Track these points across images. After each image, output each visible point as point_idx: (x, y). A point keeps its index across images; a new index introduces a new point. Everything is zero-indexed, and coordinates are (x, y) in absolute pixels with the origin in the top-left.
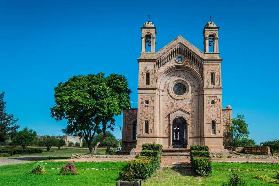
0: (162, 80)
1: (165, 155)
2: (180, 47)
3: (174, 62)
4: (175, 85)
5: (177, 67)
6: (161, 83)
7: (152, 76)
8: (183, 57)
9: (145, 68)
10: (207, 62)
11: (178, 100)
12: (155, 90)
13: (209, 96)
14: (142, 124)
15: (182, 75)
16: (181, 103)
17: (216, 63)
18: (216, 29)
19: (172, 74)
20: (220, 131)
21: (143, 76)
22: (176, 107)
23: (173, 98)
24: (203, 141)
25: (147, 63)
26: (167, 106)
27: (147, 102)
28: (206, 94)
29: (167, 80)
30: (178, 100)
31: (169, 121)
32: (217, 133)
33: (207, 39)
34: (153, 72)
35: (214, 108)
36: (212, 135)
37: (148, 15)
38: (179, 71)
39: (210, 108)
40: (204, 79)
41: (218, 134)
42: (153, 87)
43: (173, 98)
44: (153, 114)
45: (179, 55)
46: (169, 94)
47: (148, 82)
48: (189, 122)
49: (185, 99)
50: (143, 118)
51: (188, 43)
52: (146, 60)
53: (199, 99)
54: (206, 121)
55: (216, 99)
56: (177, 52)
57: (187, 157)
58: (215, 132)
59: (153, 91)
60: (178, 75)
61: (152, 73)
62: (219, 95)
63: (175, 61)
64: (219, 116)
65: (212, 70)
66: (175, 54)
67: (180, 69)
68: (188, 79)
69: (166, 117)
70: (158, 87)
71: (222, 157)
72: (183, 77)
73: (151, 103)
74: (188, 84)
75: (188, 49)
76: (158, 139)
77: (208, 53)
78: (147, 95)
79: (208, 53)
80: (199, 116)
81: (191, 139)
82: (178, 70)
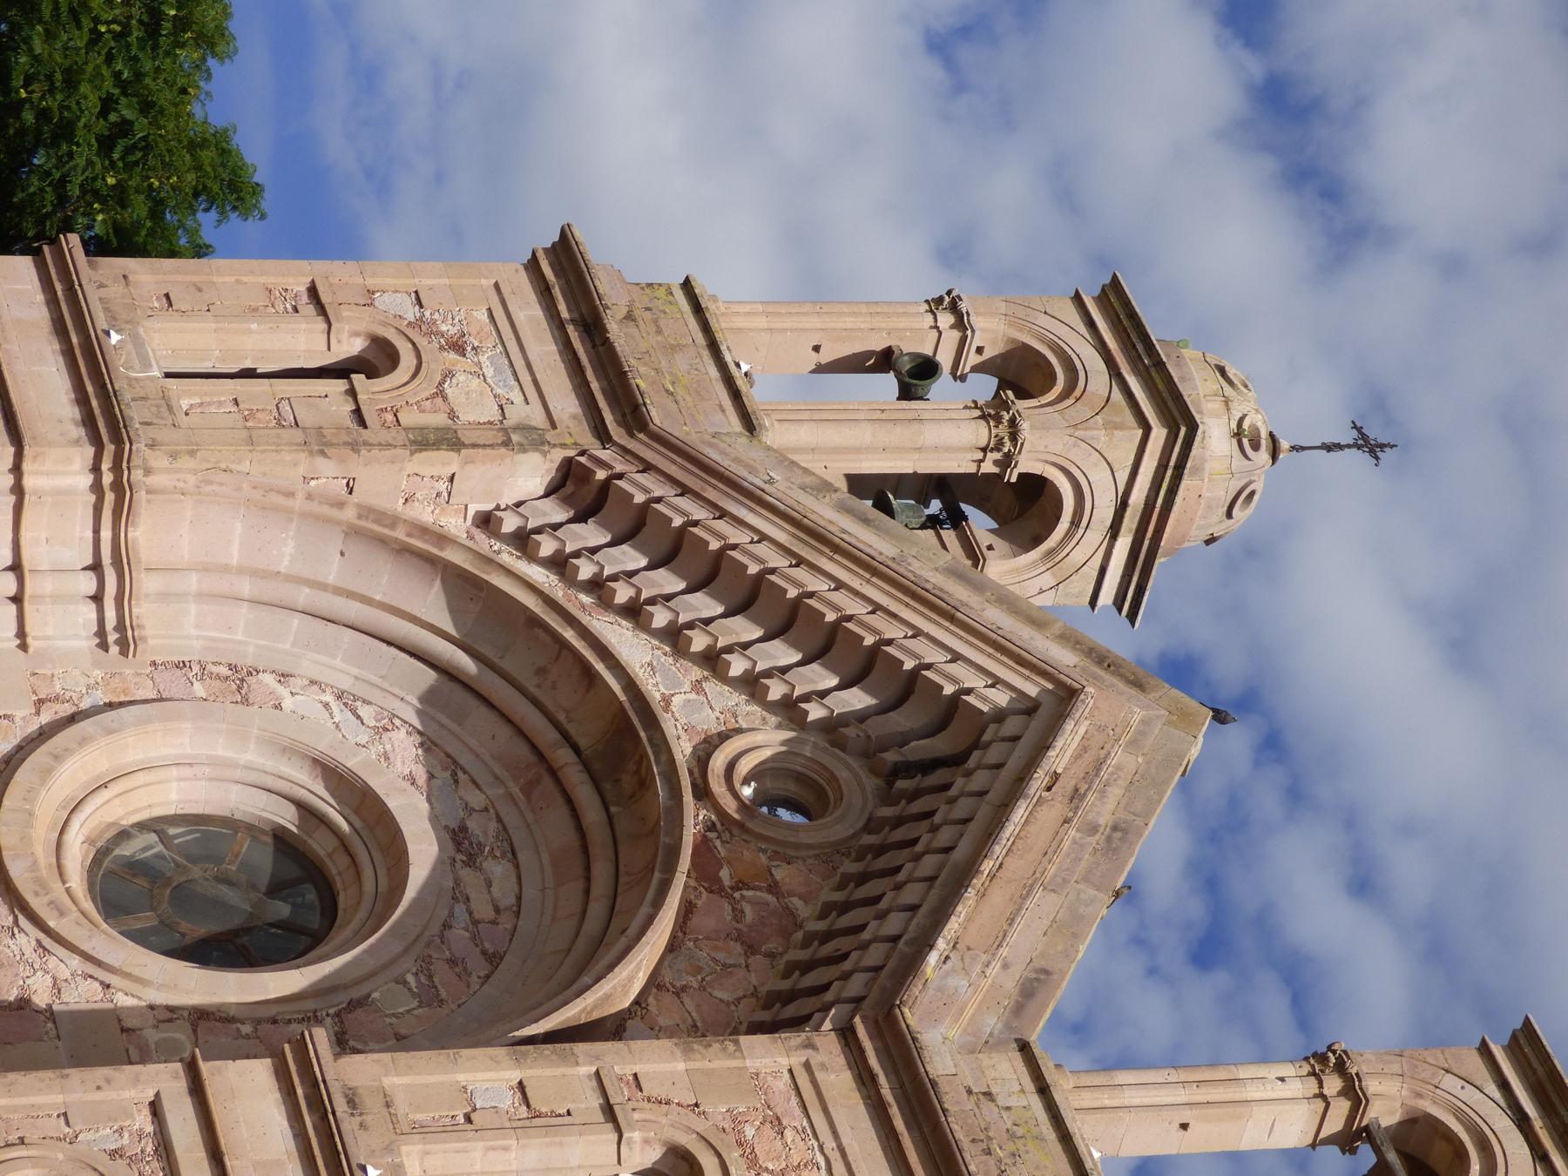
2: (999, 716)
3: (709, 722)
4: (280, 837)
6: (245, 587)
8: (837, 828)
10: (865, 1079)
12: (81, 432)
15: (504, 891)
21: (310, 310)
25: (544, 350)
28: (197, 1089)
29: (345, 683)
33: (1333, 1084)
34: (409, 418)
37: (1375, 433)
38: (558, 816)
42: (136, 414)
46: (72, 719)
49: (27, 940)
51: (1104, 808)
52: (592, 325)
56: (900, 720)
59: (72, 412)
61: (385, 401)
63: (723, 737)
65: (733, 1157)
66: (857, 699)
67: (592, 814)
68: (452, 962)
72: (459, 895)
77: (1043, 1090)
79: (1043, 1090)
82: (577, 779)
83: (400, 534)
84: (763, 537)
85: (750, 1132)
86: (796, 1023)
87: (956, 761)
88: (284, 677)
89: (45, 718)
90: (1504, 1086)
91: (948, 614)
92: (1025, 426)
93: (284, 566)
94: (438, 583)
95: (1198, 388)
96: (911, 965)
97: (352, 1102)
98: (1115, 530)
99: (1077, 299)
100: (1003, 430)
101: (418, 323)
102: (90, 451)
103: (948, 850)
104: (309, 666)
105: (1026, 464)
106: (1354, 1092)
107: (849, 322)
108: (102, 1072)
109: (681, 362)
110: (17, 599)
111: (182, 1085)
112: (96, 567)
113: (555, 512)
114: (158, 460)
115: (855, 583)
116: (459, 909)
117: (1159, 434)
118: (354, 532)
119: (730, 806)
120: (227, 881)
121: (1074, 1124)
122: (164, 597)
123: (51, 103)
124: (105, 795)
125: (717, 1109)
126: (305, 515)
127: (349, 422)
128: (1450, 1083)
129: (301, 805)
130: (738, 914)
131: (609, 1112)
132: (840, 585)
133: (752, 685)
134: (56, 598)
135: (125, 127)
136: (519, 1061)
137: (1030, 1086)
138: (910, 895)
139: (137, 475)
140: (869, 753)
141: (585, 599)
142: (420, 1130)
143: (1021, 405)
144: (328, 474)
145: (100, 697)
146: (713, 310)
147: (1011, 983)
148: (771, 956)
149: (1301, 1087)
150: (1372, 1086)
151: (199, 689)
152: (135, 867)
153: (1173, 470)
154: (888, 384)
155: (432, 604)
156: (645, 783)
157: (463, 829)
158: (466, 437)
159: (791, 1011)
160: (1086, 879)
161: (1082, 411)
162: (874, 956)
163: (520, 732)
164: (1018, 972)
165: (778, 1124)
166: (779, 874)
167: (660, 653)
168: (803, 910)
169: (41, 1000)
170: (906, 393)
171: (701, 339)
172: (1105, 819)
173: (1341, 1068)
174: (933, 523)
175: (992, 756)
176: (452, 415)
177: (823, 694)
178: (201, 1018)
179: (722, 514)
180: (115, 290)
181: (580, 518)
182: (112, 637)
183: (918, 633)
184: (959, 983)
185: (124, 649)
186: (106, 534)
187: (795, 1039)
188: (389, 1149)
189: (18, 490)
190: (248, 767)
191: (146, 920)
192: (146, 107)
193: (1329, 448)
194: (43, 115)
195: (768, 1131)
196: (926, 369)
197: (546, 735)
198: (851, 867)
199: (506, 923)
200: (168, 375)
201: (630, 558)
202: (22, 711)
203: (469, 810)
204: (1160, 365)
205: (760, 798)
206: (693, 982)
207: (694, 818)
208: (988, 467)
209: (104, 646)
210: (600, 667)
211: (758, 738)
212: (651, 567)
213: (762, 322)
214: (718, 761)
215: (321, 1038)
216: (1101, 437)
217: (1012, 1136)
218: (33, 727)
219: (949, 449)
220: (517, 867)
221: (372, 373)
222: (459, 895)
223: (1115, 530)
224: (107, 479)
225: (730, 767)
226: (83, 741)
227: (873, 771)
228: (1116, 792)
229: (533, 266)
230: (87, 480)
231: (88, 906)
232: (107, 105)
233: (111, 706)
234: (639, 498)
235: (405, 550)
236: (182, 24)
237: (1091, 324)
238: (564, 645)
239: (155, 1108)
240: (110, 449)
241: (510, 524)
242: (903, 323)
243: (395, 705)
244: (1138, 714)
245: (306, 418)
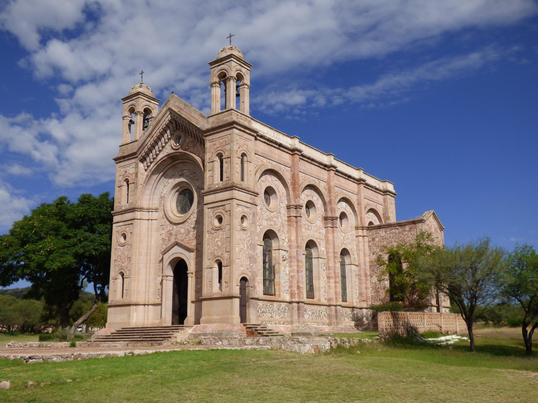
1: (104, 341)
2: (171, 117)
3: (170, 148)
4: (179, 194)
5: (171, 158)
6: (152, 196)
8: (182, 135)
10: (210, 135)
11: (179, 224)
12: (134, 212)
13: (213, 208)
14: (115, 280)
15: (187, 171)
16: (182, 231)
17: (225, 132)
18: (228, 59)
19: (170, 173)
20: (229, 284)
21: (121, 187)
22: (175, 239)
23: (171, 223)
25: (127, 163)
26: (163, 238)
27: (125, 238)
30: (179, 224)
32: (223, 289)
33: (214, 85)
34: (134, 178)
35: (220, 232)
36: (216, 289)
38: (180, 165)
39: (213, 233)
41: (226, 292)
42: (132, 207)
43: (171, 223)
44: (129, 258)
45: (177, 133)
46: (165, 215)
48: (191, 267)
49: (189, 221)
50: (117, 269)
51: (182, 106)
52: (124, 157)
54: (206, 263)
55: (223, 212)
56: (171, 127)
57: (127, 344)
58: (221, 288)
59: (131, 214)
60: (180, 173)
61: (132, 180)
62: (228, 202)
63: (172, 147)
66: (168, 132)
68: (194, 177)
69: (160, 261)
70: (145, 204)
71: (189, 342)
72: (187, 176)
74: (193, 188)
76: (142, 307)
77: (213, 116)
78: (125, 223)
79: (213, 116)
81: (193, 305)
83: (147, 180)
84: (150, 140)
85: (215, 147)
86: (204, 141)
87: (176, 122)
88: (162, 193)
89: (165, 218)
90: (215, 67)
91: (160, 121)
92: (138, 111)
93: (150, 192)
94: (153, 176)
95: (135, 91)
96: (198, 129)
97: (209, 188)
98: (150, 102)
99: (124, 103)
100: (139, 113)
101: (123, 176)
102: (136, 212)
103: (186, 124)
104: (161, 190)
105: (142, 111)
106: (215, 83)
107: (125, 129)
108: (204, 213)
109: (129, 148)
110: (152, 220)
111: (206, 206)
112: (149, 212)
113: (145, 162)
114: (137, 205)
115: (155, 131)
117: (140, 96)
118: (146, 184)
119: (179, 147)
120: (184, 200)
121: (217, 113)
122: (152, 205)
123: (96, 213)
124: (174, 212)
125: (213, 150)
126: (144, 189)
127: (134, 184)
128: (215, 72)
129: (176, 192)
130: (191, 147)
131: (212, 162)
132: (155, 133)
133: (166, 143)
134: (152, 216)
135: (99, 206)
136: (206, 171)
137: (212, 117)
138: (191, 128)
139: (139, 207)
140: (174, 131)
141: (155, 160)
142: (213, 181)
143: (136, 111)
144: (140, 187)
145: (163, 212)
146: (123, 144)
147: (201, 118)
148: (196, 143)
149: (214, 89)
150: (214, 81)
151: (163, 202)
152: (181, 209)
153: (144, 95)
154: (132, 125)
155: (155, 177)
156: (176, 155)
158: (136, 172)
159: (202, 142)
160: (190, 109)
161: (137, 104)
162: (197, 133)
163: (170, 168)
164: (200, 117)
165: (215, 144)
166: (187, 142)
167: (162, 153)
169: (195, 219)
170: (134, 123)
171: (126, 145)
172: (184, 106)
173: (212, 84)
174: (148, 122)
175: (176, 118)
176: (134, 173)
177: (167, 135)
178: (199, 203)
179: (147, 145)
180: (118, 208)
181: (146, 160)
182: (156, 210)
183: (161, 124)
184: (201, 124)
185: (158, 209)
186: (145, 210)
187: (206, 142)
188: (215, 185)
189: (140, 219)
190: (172, 197)
191: (187, 209)
192: (97, 203)
193: (142, 77)
194: (97, 214)
195: (215, 145)
196: (131, 121)
197: (170, 166)
198: (187, 134)
199: (190, 171)
200: (128, 203)
201: (151, 155)
202: (164, 220)
204: (132, 95)
205: (179, 143)
206: (198, 152)
207: (180, 150)
208: (143, 115)
209: (157, 211)
210: (163, 159)
211: (172, 143)
212: (152, 153)
213: (124, 139)
214: (174, 147)
215: (202, 191)
216: (140, 102)
217: (218, 120)
218: (166, 219)
219: (140, 119)
220: (184, 170)
221: (129, 181)
222: (187, 176)
223: (150, 102)
224: (139, 210)
225: (175, 146)
226: (168, 214)
227: (176, 131)
228: (181, 105)
229: (117, 163)
230: (139, 212)
231: (186, 214)
232: (97, 208)
233: (164, 211)
234: (144, 154)
235: (149, 179)
236: (88, 199)
237: (127, 102)
238: (160, 163)
239: (209, 208)
240: (136, 209)
241: (146, 168)
242: (125, 123)
243: (165, 181)
244: (172, 101)
245: (133, 189)
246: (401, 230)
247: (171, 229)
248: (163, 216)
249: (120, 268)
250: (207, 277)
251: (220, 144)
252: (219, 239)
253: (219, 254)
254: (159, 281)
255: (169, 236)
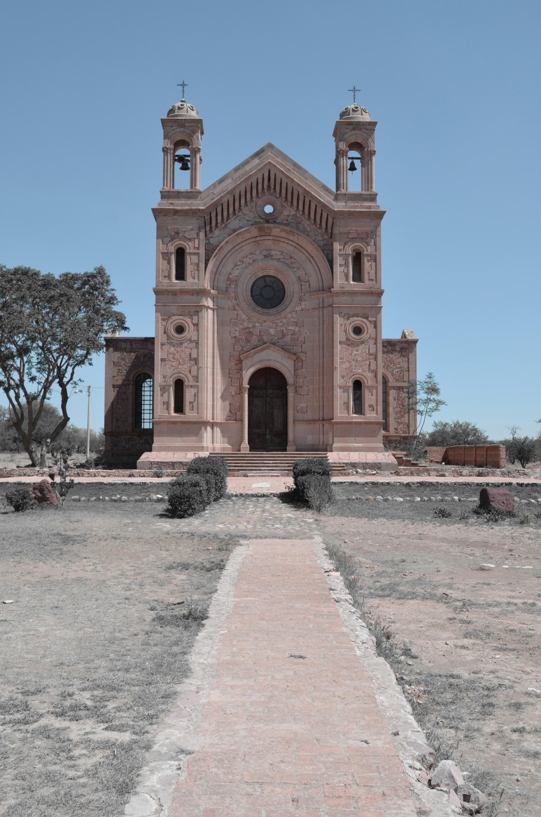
0: (220, 268)
6: (217, 276)
7: (193, 257)
9: (173, 234)
16: (272, 331)
24: (331, 433)
26: (235, 337)
31: (241, 379)
37: (181, 83)
40: (334, 266)
44: (196, 361)
47: (181, 275)
53: (321, 319)
60: (265, 253)
61: (192, 248)
64: (373, 367)
68: (292, 263)
72: (279, 260)
73: (190, 333)
75: (292, 180)
80: (321, 366)
85: (350, 237)
97: (343, 288)
116: (283, 260)
157: (265, 255)
168: (293, 212)
197: (254, 240)
203: (261, 254)
246: (390, 348)
247: (251, 326)
248: (234, 307)
249: (176, 371)
250: (341, 397)
251: (359, 234)
252: (358, 353)
253: (360, 371)
254: (231, 393)
255: (246, 335)
